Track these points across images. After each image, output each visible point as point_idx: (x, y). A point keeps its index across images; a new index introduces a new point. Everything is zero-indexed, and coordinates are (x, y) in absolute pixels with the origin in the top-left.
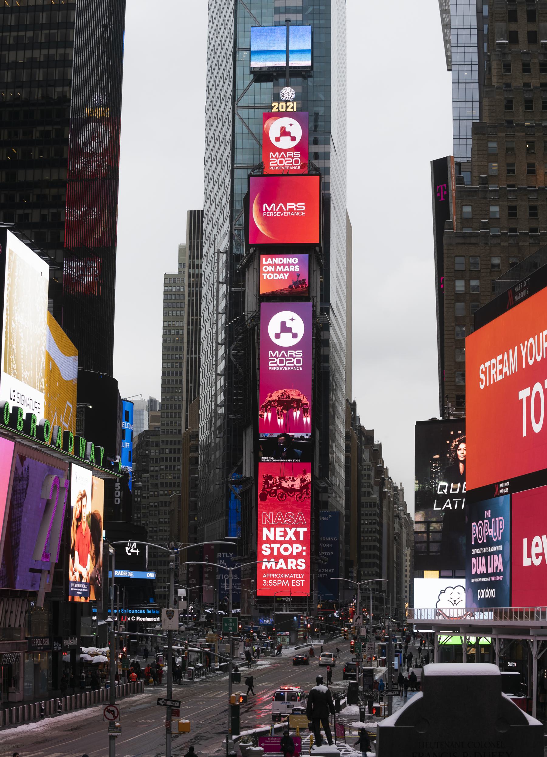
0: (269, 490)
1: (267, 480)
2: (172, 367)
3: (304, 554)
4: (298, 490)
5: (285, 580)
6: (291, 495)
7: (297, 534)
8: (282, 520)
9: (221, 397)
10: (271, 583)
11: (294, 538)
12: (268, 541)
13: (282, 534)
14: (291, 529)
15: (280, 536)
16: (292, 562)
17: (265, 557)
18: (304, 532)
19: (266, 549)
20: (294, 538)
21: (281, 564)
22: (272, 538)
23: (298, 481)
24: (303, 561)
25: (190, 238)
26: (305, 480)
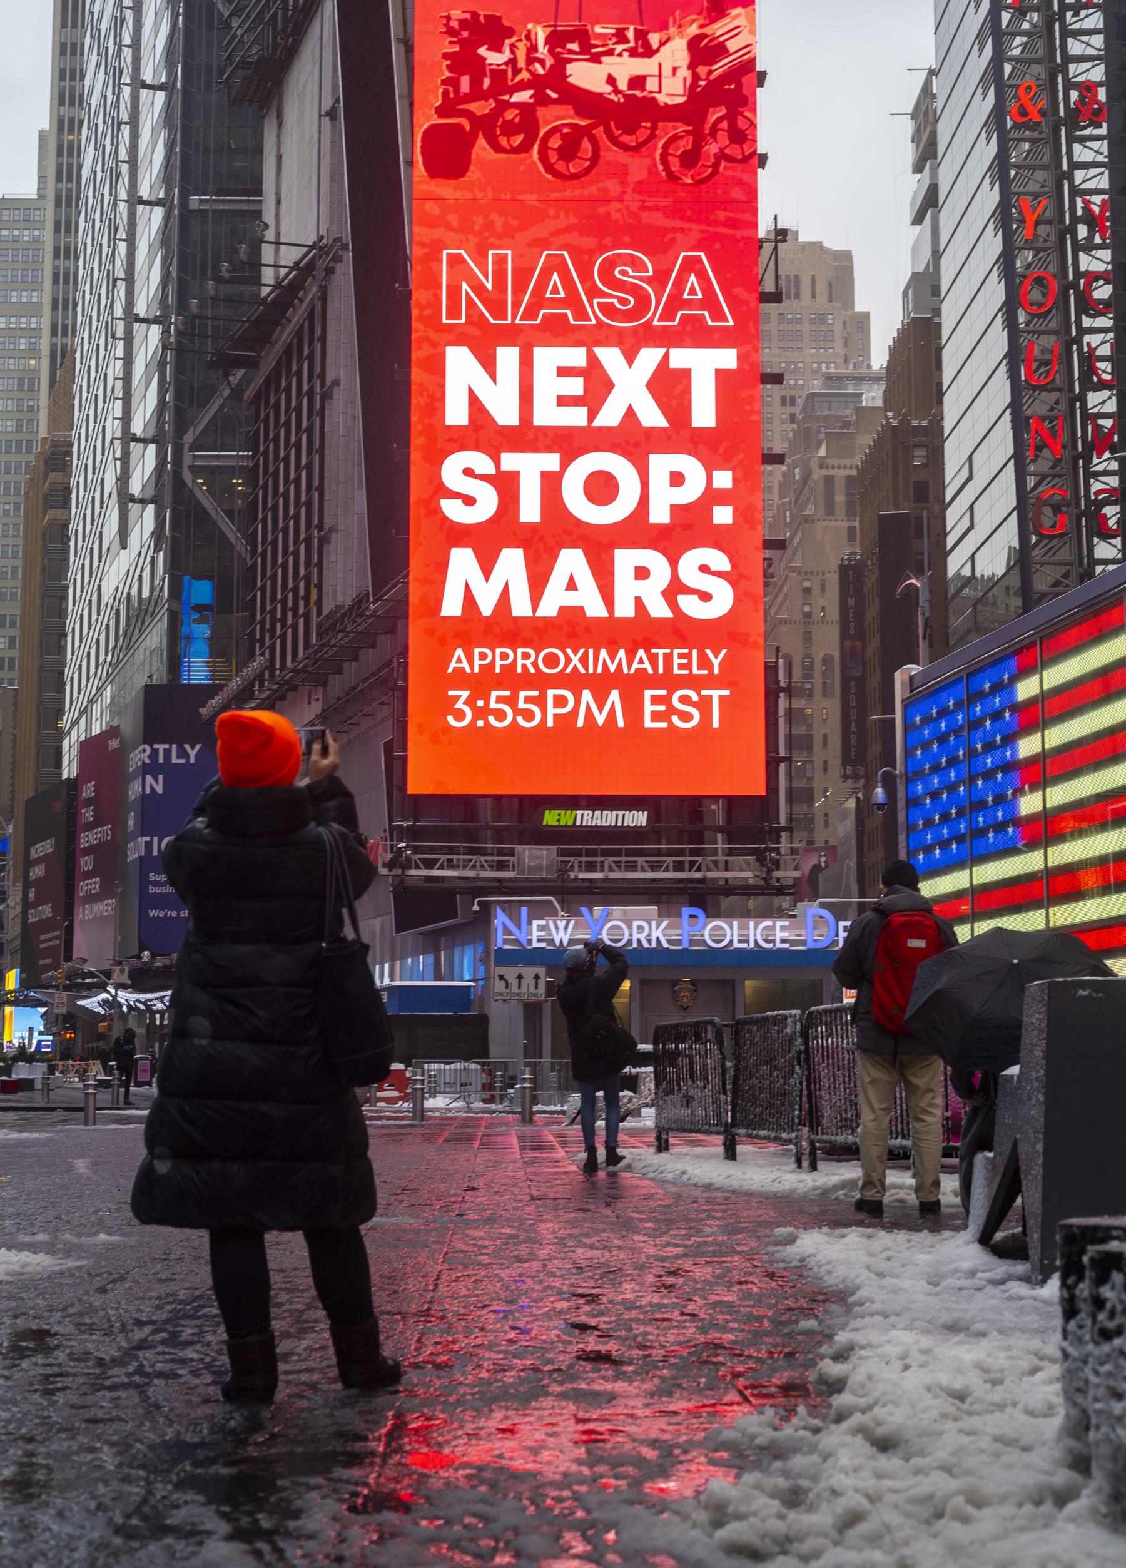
0: (481, 108)
1: (468, 49)
2: (19, 429)
3: (723, 515)
4: (672, 113)
5: (601, 685)
6: (630, 140)
7: (670, 387)
8: (572, 300)
9: (146, 461)
10: (506, 712)
11: (652, 416)
12: (482, 432)
13: (575, 386)
14: (630, 359)
15: (563, 401)
16: (642, 573)
17: (461, 535)
18: (719, 372)
19: (465, 487)
20: (652, 416)
21: (571, 585)
22: (506, 414)
23: (675, 53)
24: (719, 560)
25: (64, 25)
26: (720, 50)
